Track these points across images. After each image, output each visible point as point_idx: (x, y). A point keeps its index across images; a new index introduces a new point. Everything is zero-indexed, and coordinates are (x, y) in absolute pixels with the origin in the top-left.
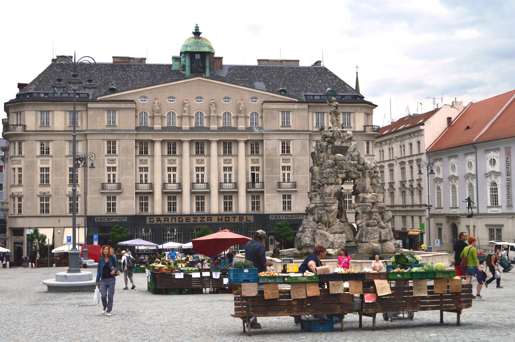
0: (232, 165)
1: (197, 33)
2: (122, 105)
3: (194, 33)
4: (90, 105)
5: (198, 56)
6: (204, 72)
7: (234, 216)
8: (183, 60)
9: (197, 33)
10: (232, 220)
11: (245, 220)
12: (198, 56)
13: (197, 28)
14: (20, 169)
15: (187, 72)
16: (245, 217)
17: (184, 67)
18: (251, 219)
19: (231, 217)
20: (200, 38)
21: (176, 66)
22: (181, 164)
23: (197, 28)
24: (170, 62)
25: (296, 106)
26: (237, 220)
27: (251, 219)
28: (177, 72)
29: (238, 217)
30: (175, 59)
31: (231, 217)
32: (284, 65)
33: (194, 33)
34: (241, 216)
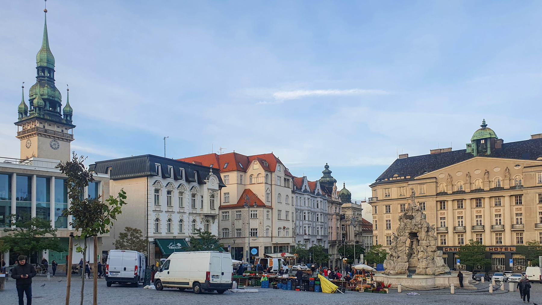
0: (501, 213)
1: (484, 126)
3: (482, 126)
5: (483, 142)
6: (487, 151)
7: (501, 247)
8: (472, 145)
9: (484, 126)
10: (499, 250)
11: (509, 250)
12: (483, 142)
13: (484, 122)
14: (376, 221)
16: (509, 248)
17: (473, 150)
18: (514, 249)
19: (498, 248)
21: (469, 151)
22: (465, 214)
23: (484, 122)
24: (465, 148)
26: (503, 250)
27: (514, 249)
28: (469, 154)
29: (504, 248)
30: (469, 146)
31: (498, 248)
33: (482, 126)
34: (506, 247)
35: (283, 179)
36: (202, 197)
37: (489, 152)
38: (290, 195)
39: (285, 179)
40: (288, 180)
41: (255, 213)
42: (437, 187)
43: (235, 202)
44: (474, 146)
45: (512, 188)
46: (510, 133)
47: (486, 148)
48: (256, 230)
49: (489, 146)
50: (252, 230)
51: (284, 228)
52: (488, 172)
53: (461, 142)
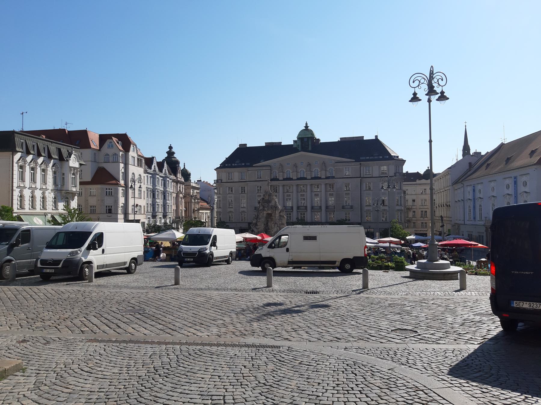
1: (307, 127)
2: (264, 168)
4: (250, 169)
5: (306, 140)
9: (307, 127)
12: (306, 140)
13: (306, 124)
15: (300, 149)
20: (308, 130)
23: (306, 124)
25: (353, 164)
28: (296, 148)
30: (295, 141)
32: (355, 139)
35: (136, 159)
36: (63, 174)
37: (310, 149)
38: (143, 175)
39: (138, 159)
40: (141, 159)
41: (110, 191)
42: (271, 173)
43: (89, 179)
44: (299, 143)
45: (327, 178)
46: (326, 134)
47: (308, 145)
48: (111, 207)
49: (310, 143)
50: (106, 207)
51: (137, 205)
52: (310, 164)
53: (288, 139)
